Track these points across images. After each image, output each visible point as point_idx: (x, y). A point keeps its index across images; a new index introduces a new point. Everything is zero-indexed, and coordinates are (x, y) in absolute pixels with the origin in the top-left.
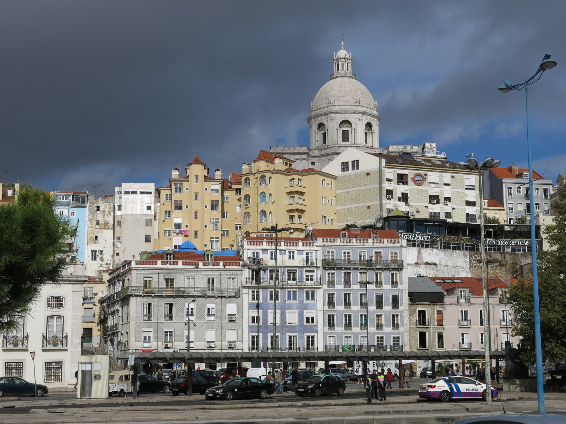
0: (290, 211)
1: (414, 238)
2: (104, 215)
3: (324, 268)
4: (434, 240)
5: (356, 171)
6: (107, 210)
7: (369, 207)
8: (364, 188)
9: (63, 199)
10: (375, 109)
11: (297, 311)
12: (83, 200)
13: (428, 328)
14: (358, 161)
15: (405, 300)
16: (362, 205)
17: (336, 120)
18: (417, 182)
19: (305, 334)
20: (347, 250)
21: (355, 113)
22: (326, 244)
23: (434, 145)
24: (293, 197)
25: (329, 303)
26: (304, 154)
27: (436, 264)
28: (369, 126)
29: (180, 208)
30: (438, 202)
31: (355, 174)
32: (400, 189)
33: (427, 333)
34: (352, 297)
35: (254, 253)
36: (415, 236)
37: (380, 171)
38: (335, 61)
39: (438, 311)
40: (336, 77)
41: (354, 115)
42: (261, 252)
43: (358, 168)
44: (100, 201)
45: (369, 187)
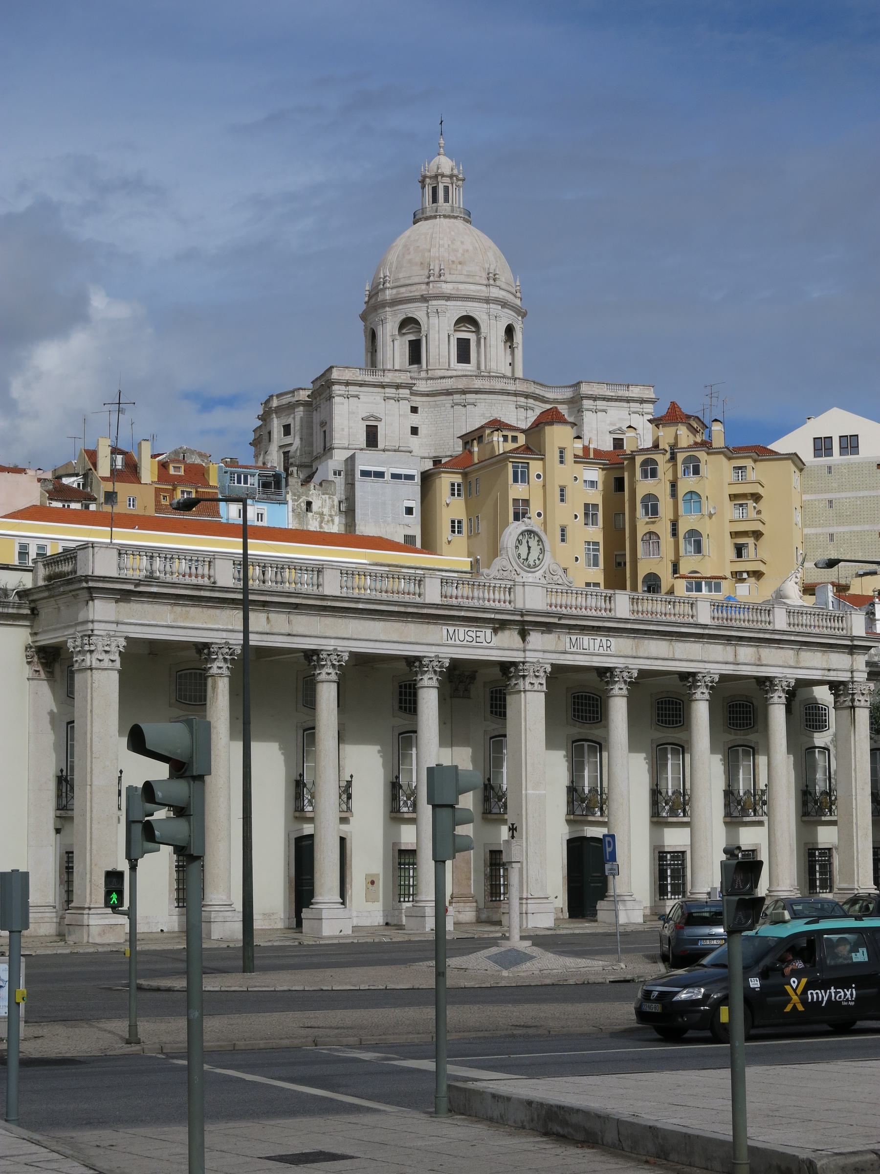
0: (735, 534)
2: (321, 522)
6: (326, 511)
9: (239, 482)
12: (278, 486)
16: (867, 527)
17: (448, 315)
21: (487, 301)
24: (741, 505)
26: (405, 387)
28: (510, 331)
41: (485, 306)
44: (312, 491)
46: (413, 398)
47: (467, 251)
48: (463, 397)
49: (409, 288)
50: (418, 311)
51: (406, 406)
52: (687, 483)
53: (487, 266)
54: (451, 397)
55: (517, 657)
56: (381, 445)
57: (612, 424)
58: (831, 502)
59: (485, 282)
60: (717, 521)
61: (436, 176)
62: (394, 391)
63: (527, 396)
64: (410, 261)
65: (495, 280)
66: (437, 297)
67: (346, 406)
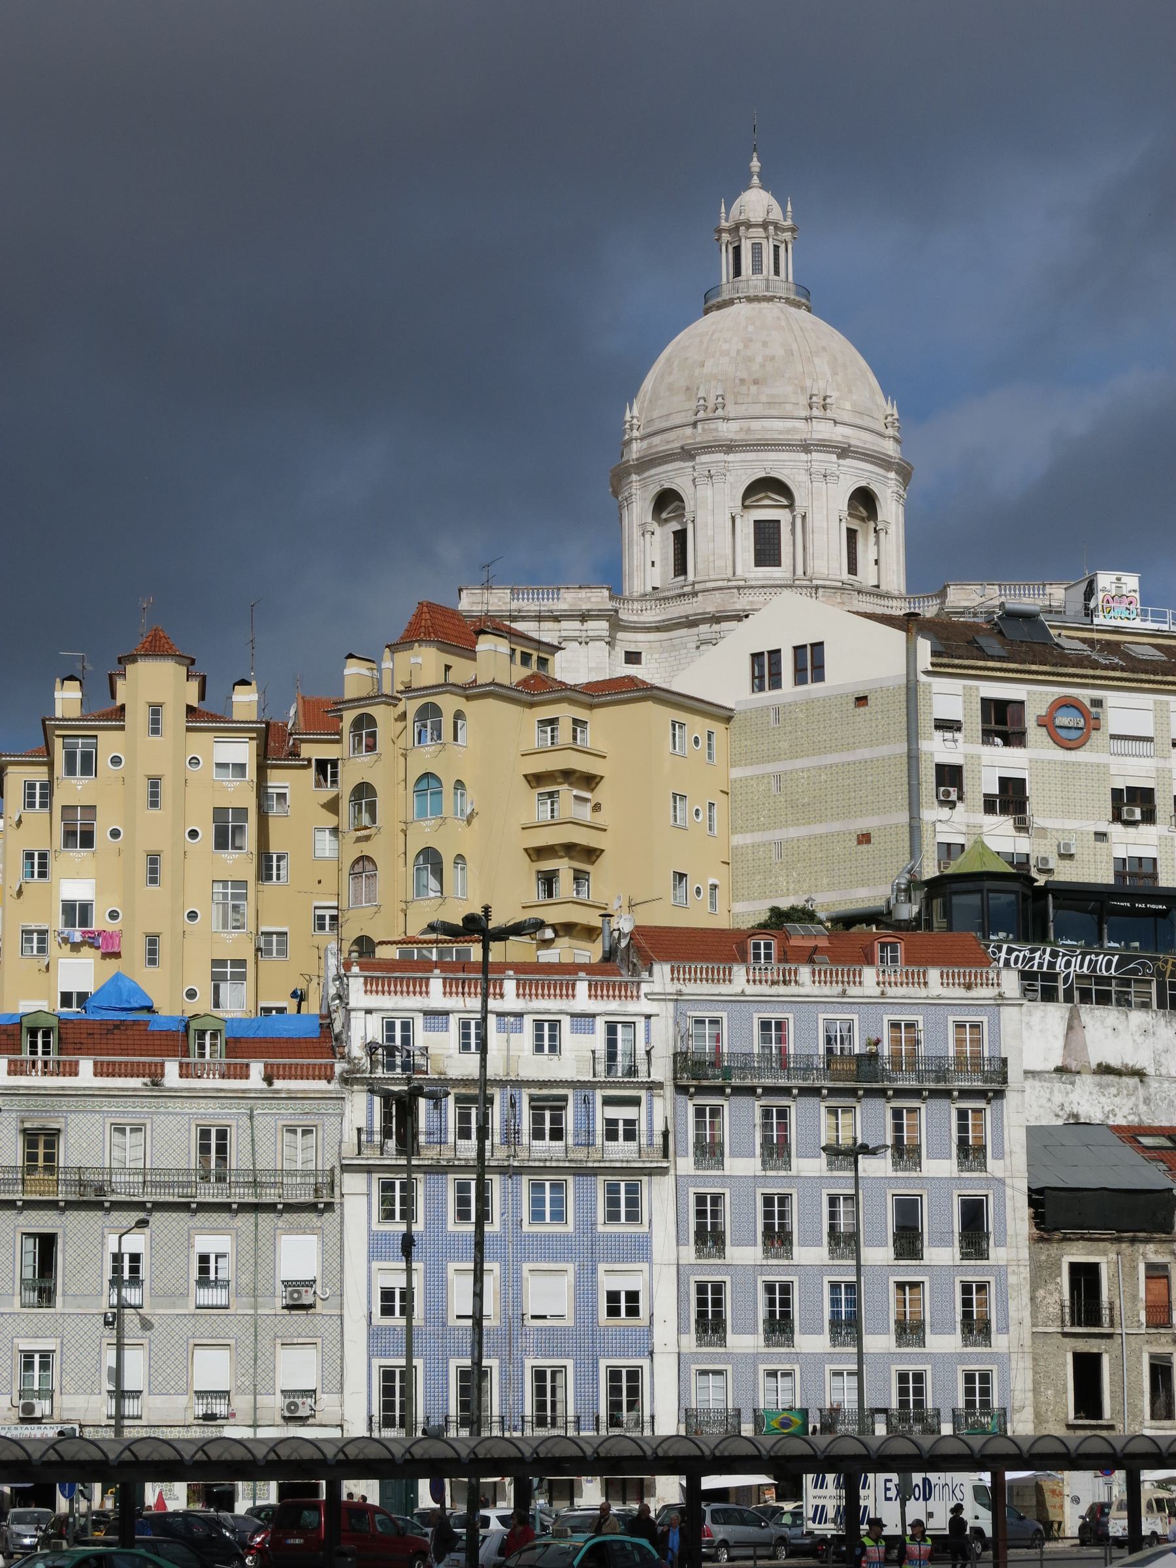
0: (538, 853)
1: (1052, 965)
3: (681, 1089)
4: (1134, 971)
5: (812, 688)
7: (864, 839)
10: (890, 432)
11: (570, 1267)
13: (1109, 1336)
14: (818, 646)
15: (1013, 1219)
16: (836, 826)
18: (1063, 733)
19: (603, 1363)
20: (774, 1015)
21: (806, 447)
22: (690, 988)
23: (1131, 582)
24: (551, 795)
25: (701, 1235)
26: (598, 617)
27: (1139, 1074)
28: (864, 501)
29: (87, 840)
30: (1149, 817)
31: (809, 703)
32: (991, 764)
33: (1106, 1361)
34: (795, 1205)
35: (390, 1026)
36: (1054, 954)
37: (911, 689)
38: (725, 237)
39: (1150, 1267)
40: (730, 302)
41: (803, 456)
42: (419, 1022)
43: (819, 676)
45: (864, 753)
47: (773, 358)
48: (716, 627)
49: (666, 436)
53: (808, 383)
54: (694, 630)
59: (804, 413)
62: (576, 624)
65: (824, 407)
66: (708, 449)
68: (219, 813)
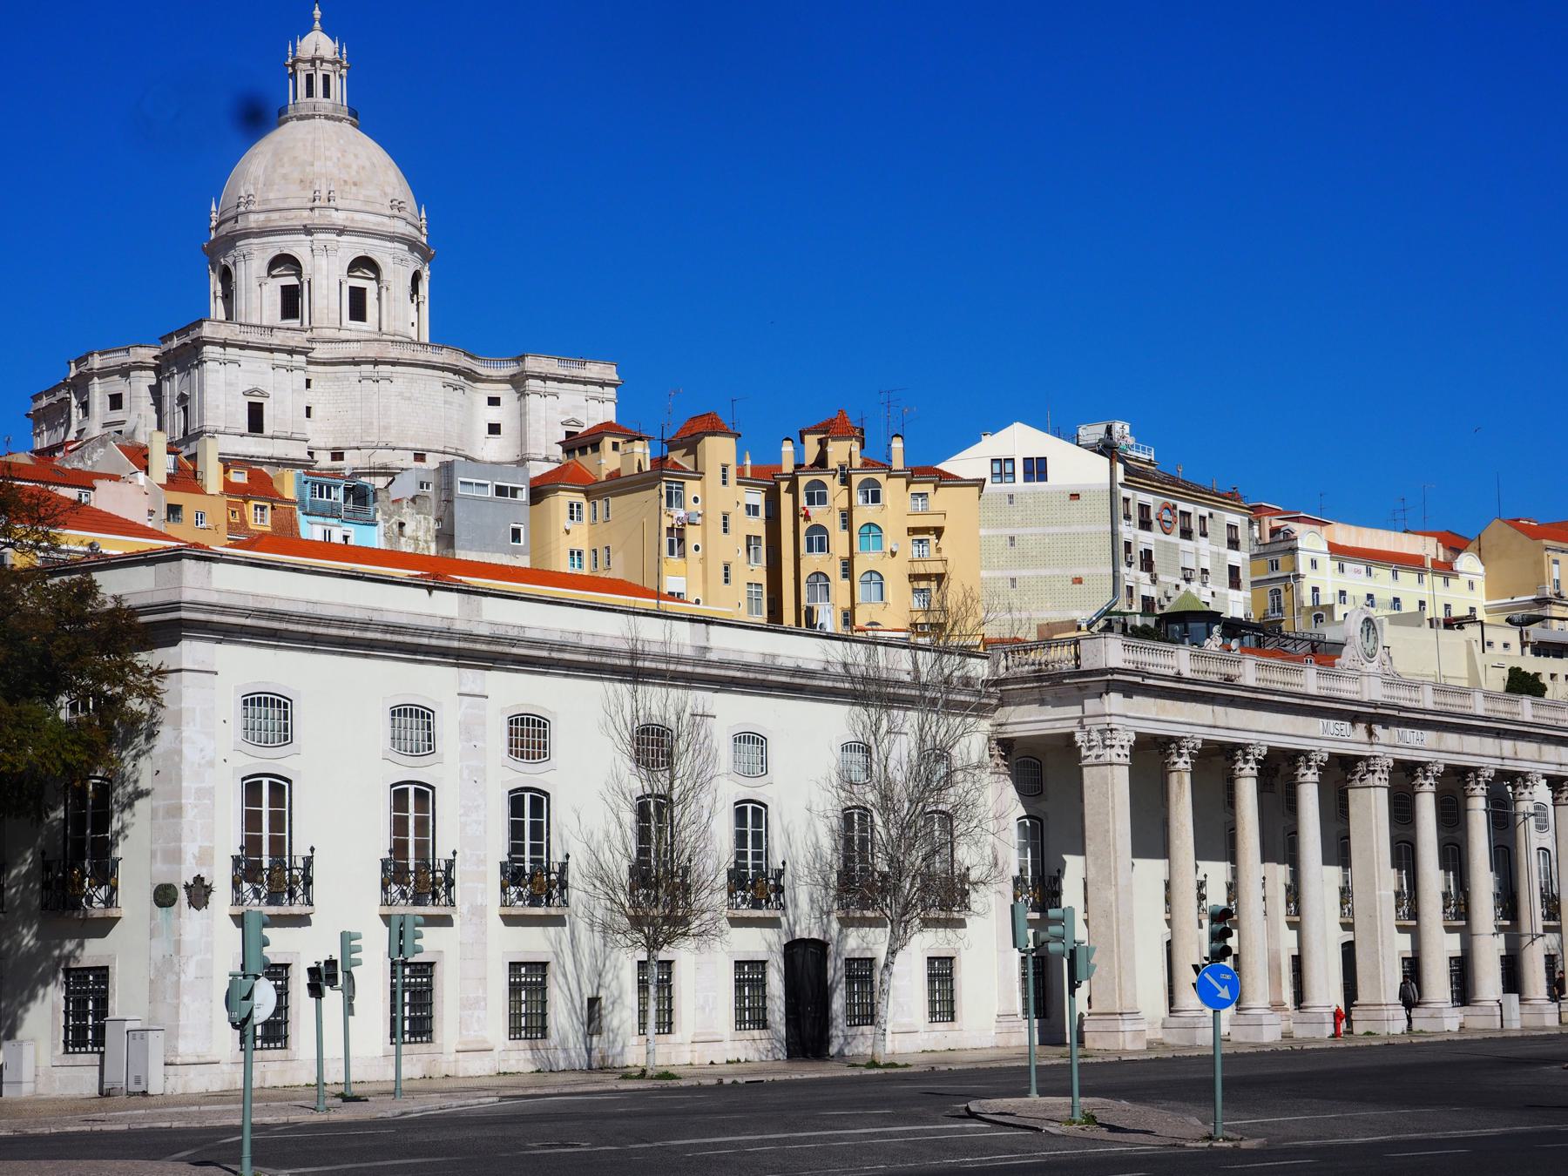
6: (421, 534)
7: (1078, 581)
8: (1063, 530)
9: (321, 496)
16: (1057, 571)
21: (392, 238)
23: (1127, 428)
24: (921, 541)
28: (416, 277)
46: (311, 368)
49: (285, 214)
50: (298, 247)
51: (300, 377)
52: (864, 513)
55: (1366, 750)
56: (267, 430)
57: (564, 413)
58: (1012, 539)
59: (389, 212)
60: (893, 559)
61: (313, 61)
63: (456, 371)
64: (285, 177)
67: (222, 376)
68: (749, 537)
